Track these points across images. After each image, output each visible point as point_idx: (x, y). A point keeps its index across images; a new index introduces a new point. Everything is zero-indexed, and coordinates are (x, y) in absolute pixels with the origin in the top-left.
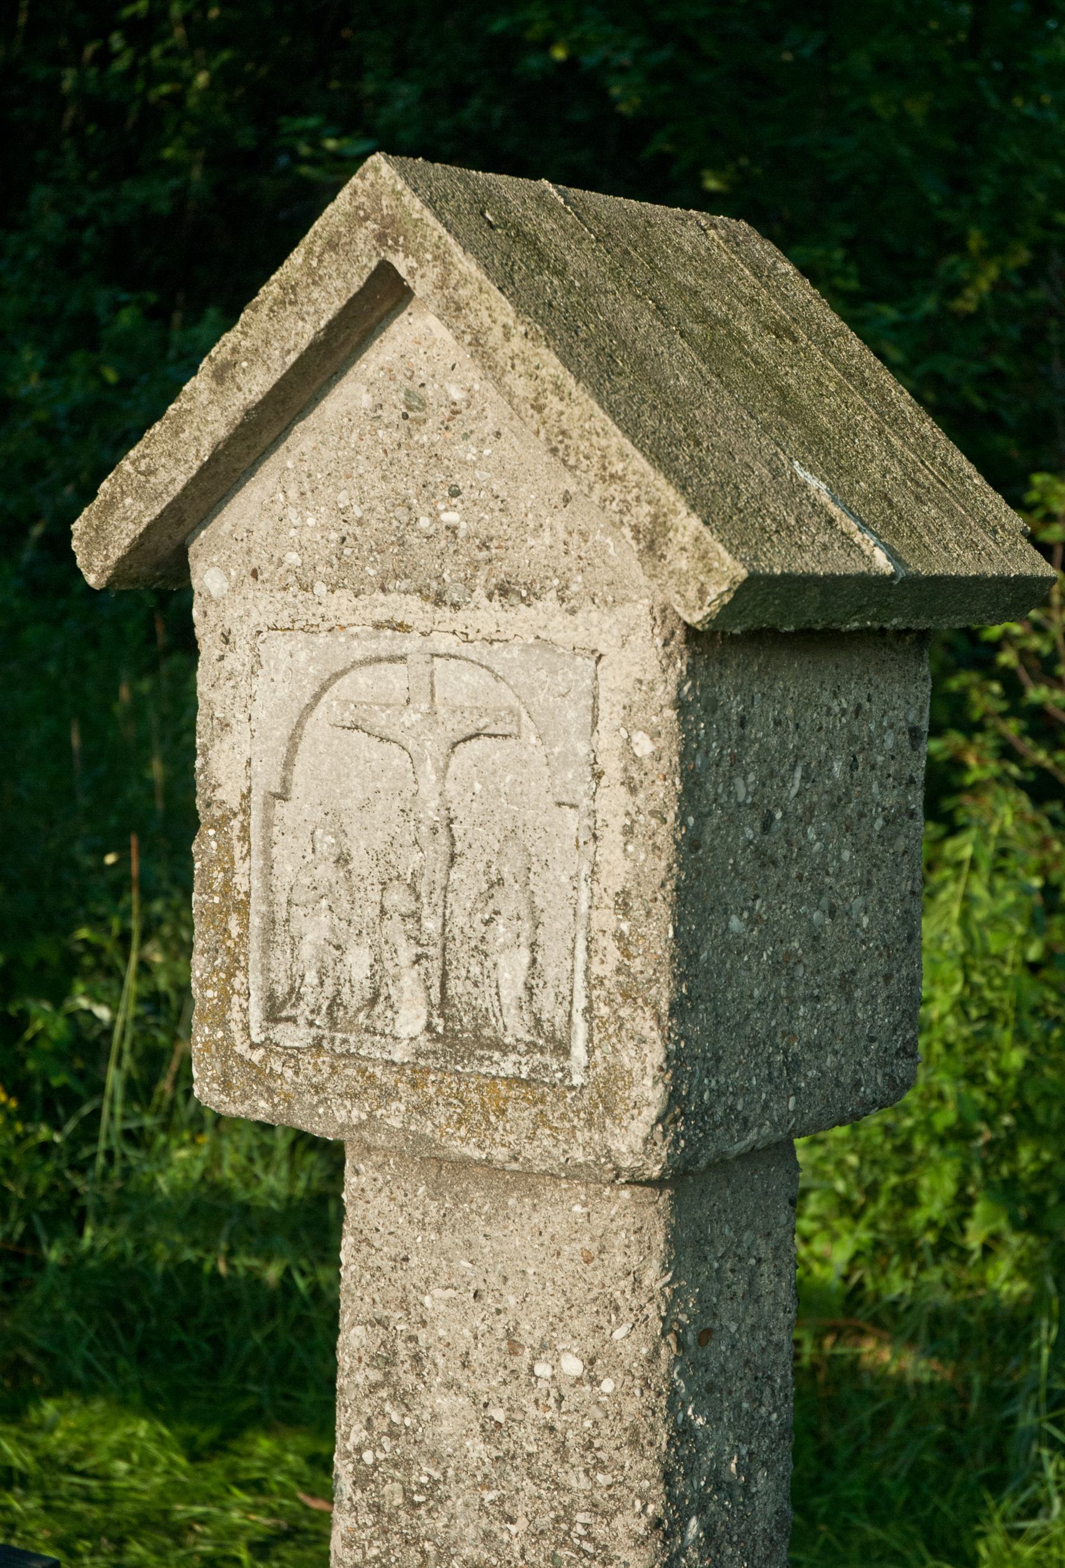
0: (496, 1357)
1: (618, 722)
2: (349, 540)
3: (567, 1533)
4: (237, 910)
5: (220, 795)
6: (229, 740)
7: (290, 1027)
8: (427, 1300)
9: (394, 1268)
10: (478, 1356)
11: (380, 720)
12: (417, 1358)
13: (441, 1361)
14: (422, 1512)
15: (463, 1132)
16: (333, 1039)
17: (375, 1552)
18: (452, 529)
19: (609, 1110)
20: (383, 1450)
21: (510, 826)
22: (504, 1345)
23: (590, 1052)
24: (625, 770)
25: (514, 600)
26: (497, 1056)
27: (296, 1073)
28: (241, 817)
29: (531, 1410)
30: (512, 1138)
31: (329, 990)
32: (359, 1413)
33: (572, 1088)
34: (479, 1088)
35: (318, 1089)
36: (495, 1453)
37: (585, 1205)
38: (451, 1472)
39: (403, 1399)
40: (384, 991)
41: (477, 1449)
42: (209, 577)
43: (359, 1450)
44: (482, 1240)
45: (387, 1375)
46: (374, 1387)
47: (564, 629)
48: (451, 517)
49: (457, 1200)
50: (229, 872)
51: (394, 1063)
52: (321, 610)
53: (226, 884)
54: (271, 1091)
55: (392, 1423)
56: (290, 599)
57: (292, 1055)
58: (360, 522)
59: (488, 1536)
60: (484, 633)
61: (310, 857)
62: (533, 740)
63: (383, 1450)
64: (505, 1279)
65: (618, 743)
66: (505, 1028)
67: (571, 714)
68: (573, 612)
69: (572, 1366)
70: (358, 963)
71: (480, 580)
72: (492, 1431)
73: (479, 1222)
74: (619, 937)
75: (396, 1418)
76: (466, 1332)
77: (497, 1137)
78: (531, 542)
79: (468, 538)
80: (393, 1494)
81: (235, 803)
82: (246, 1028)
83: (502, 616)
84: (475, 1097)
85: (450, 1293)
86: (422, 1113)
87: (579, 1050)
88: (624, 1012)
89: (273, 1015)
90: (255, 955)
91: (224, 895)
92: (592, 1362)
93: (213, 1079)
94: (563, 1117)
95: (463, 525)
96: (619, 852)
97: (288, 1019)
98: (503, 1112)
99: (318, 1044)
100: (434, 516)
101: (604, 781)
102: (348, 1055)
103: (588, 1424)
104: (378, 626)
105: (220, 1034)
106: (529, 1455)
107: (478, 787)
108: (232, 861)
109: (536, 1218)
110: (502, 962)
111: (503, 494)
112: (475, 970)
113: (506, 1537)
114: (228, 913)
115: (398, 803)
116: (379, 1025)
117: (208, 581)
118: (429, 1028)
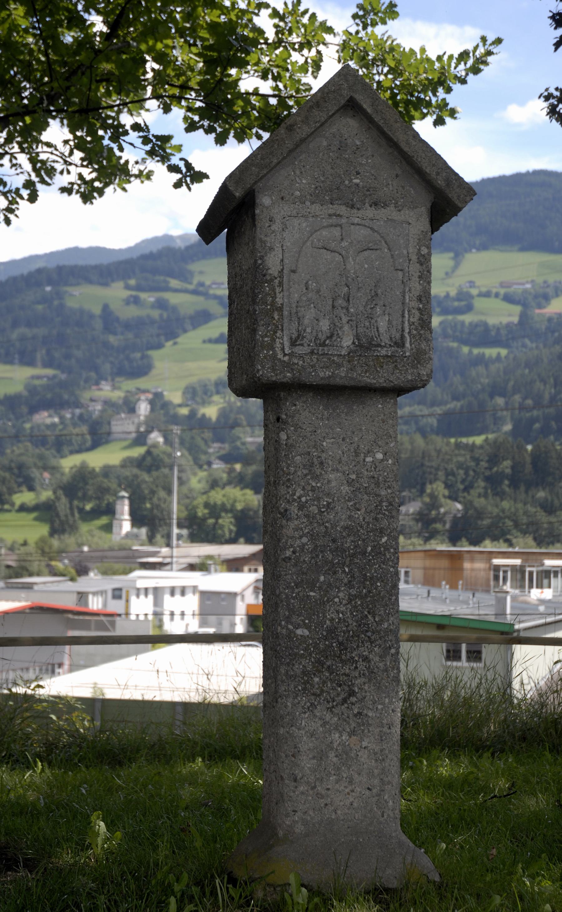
0: (351, 458)
1: (415, 244)
2: (319, 188)
3: (381, 509)
4: (277, 309)
5: (270, 272)
6: (273, 253)
7: (301, 348)
8: (324, 444)
9: (311, 435)
10: (344, 459)
11: (333, 245)
12: (321, 463)
13: (330, 463)
14: (325, 514)
15: (368, 374)
16: (318, 350)
17: (307, 531)
18: (357, 185)
19: (419, 363)
20: (309, 496)
21: (378, 277)
22: (353, 454)
23: (411, 345)
24: (418, 258)
25: (379, 207)
26: (379, 349)
27: (304, 362)
28: (278, 279)
29: (366, 473)
30: (385, 375)
31: (314, 334)
32: (299, 485)
33: (405, 357)
34: (373, 360)
35: (312, 366)
36: (352, 489)
37: (382, 404)
38: (335, 499)
39: (317, 478)
40: (336, 333)
41: (345, 489)
42: (265, 200)
43: (299, 498)
44: (344, 421)
45: (310, 471)
46: (306, 475)
47: (395, 215)
48: (357, 181)
49: (334, 410)
50: (274, 297)
51: (341, 355)
52: (309, 210)
53: (273, 301)
54: (292, 369)
55: (313, 486)
56: (296, 206)
57: (301, 357)
58: (323, 182)
59: (350, 517)
60: (369, 217)
61: (305, 291)
62: (386, 250)
63: (309, 496)
64: (353, 433)
65: (416, 250)
66: (381, 340)
67: (402, 241)
68: (400, 211)
69: (380, 456)
70: (325, 325)
71: (367, 201)
72: (350, 483)
73: (343, 415)
74: (419, 309)
75: (314, 484)
76: (340, 452)
77: (380, 375)
78: (385, 189)
79: (363, 187)
80: (314, 509)
81: (276, 274)
82: (283, 349)
83: (375, 212)
84: (372, 363)
85: (333, 440)
86: (352, 370)
87: (408, 345)
88: (422, 332)
89: (293, 343)
90: (285, 325)
91: (271, 305)
92: (386, 454)
93: (268, 368)
94: (403, 366)
95: (361, 183)
96: (417, 284)
97: (299, 345)
98: (382, 367)
99: (312, 352)
100: (351, 181)
101: (411, 262)
102: (324, 354)
103: (386, 474)
104: (330, 215)
105: (271, 352)
106: (366, 487)
107: (366, 266)
108: (275, 294)
109: (364, 411)
110: (379, 320)
111: (375, 174)
112: (367, 324)
113: (357, 516)
114: (273, 311)
115: (338, 272)
116: (335, 343)
117: (264, 201)
118: (354, 343)
